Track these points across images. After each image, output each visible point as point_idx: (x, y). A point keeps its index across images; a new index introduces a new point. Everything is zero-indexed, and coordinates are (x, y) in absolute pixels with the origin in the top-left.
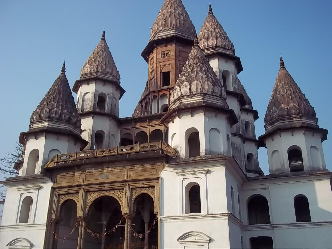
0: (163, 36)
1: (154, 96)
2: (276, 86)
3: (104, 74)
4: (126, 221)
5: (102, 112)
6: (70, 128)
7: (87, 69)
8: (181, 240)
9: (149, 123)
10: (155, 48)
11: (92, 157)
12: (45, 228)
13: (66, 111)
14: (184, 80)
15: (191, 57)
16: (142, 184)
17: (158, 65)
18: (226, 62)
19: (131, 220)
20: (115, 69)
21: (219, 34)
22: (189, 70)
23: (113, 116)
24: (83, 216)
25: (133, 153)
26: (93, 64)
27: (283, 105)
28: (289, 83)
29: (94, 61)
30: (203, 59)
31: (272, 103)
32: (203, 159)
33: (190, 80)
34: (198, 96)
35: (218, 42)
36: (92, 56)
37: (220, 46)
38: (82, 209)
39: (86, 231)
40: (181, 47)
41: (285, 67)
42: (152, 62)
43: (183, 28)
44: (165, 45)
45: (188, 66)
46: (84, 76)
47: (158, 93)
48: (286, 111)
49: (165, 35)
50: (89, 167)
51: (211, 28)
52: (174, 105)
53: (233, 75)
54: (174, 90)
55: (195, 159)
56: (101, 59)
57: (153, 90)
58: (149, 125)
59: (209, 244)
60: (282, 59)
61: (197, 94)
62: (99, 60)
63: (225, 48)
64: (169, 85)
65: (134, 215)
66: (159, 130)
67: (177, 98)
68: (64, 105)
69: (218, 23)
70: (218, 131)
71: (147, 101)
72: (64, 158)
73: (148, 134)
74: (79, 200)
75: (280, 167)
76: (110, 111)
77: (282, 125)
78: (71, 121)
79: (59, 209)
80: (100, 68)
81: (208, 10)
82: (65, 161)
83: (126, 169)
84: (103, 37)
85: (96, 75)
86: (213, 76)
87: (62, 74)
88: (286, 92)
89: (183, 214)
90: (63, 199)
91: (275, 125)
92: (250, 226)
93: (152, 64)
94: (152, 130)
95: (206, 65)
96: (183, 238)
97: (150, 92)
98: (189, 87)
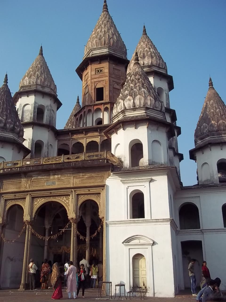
0: (98, 53)
1: (88, 110)
2: (206, 105)
3: (43, 87)
4: (72, 225)
5: (41, 123)
6: (14, 137)
7: (27, 82)
8: (126, 243)
9: (85, 135)
10: (90, 65)
11: (38, 164)
13: (10, 120)
14: (127, 94)
15: (133, 73)
16: (88, 191)
17: (92, 81)
18: (160, 80)
19: (76, 224)
20: (53, 82)
21: (154, 53)
22: (131, 85)
23: (51, 127)
24: (30, 220)
25: (79, 161)
26: (33, 77)
27: (213, 122)
28: (218, 102)
29: (33, 75)
30: (143, 75)
31: (202, 120)
32: (147, 168)
33: (133, 94)
34: (141, 110)
35: (153, 61)
36: (31, 69)
37: (155, 65)
38: (29, 214)
39: (33, 234)
40: (114, 65)
41: (213, 87)
42: (86, 78)
43: (116, 47)
44: (99, 62)
45: (130, 81)
46: (23, 88)
47: (93, 107)
48: (216, 127)
49: (99, 53)
50: (36, 174)
51: (146, 48)
52: (117, 118)
53: (166, 93)
54: (118, 104)
55: (139, 169)
56: (40, 73)
57: (87, 104)
58: (85, 136)
59: (153, 246)
60: (210, 80)
61: (140, 108)
62: (38, 74)
63: (159, 67)
64: (103, 100)
65: (79, 220)
66: (95, 141)
67: (121, 111)
68: (8, 114)
69: (152, 43)
70: (159, 143)
71: (81, 115)
72: (10, 165)
73: (85, 145)
74: (26, 205)
75: (209, 178)
76: (48, 122)
77: (212, 140)
78: (15, 130)
79: (6, 213)
80: (39, 81)
81: (143, 31)
82: (11, 168)
83: (72, 177)
84: (41, 52)
85: (35, 88)
86: (154, 91)
87: (4, 85)
88: (216, 110)
89: (128, 219)
90: (10, 204)
91: (205, 140)
92: (181, 231)
93: (86, 80)
94: (89, 142)
95: (148, 82)
96: (127, 241)
97: (85, 106)
98: (132, 101)
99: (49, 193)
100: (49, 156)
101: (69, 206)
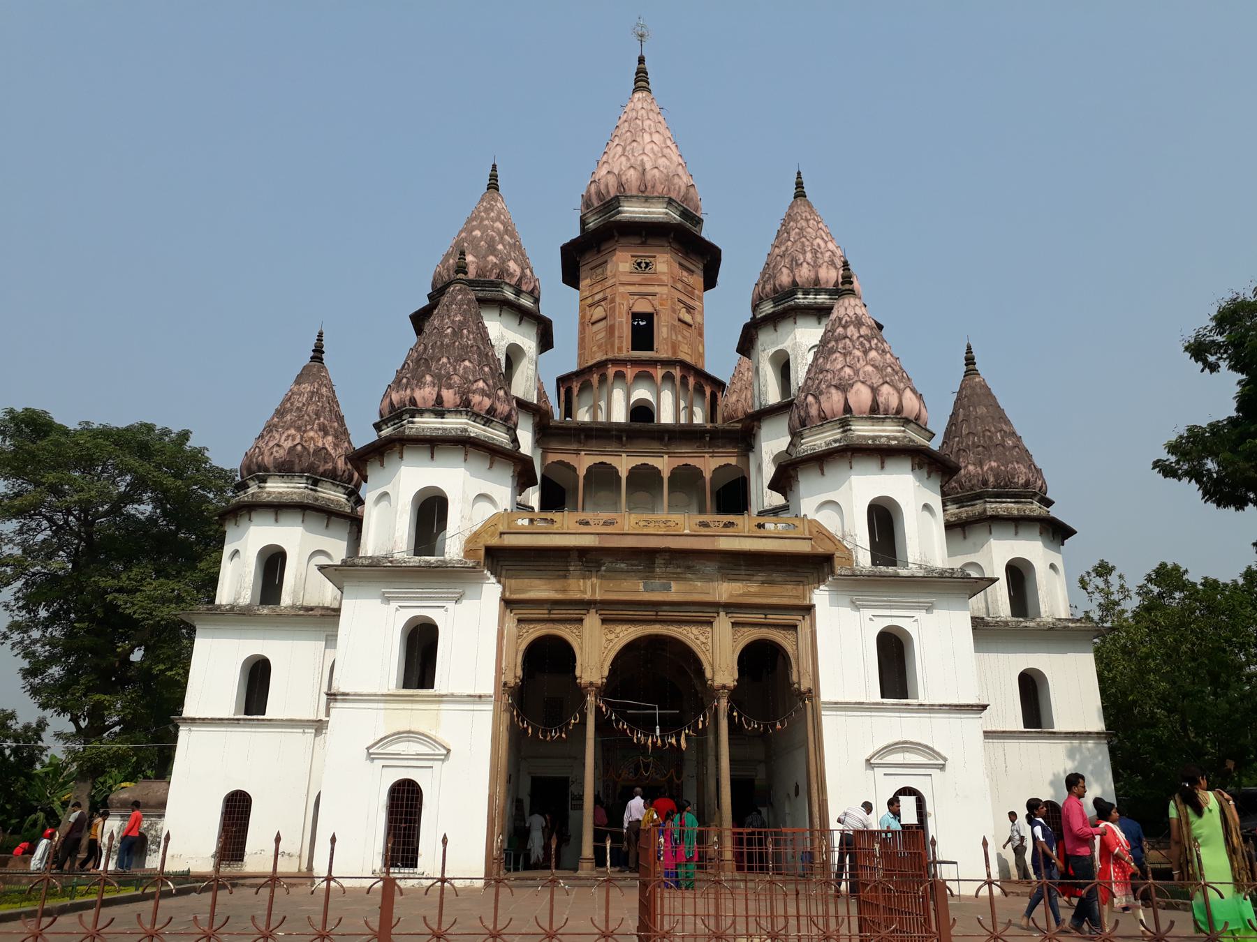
12: (491, 707)
16: (763, 616)
24: (600, 682)
64: (652, 349)
73: (623, 474)
99: (654, 613)
100: (374, 473)
101: (707, 653)
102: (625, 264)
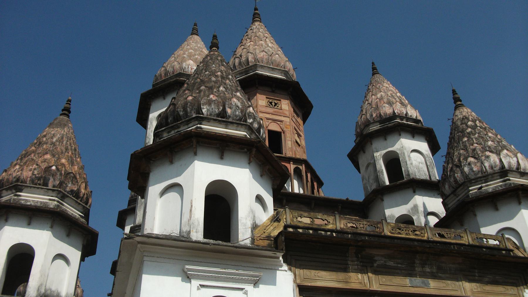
40: (293, 102)
102: (262, 101)
